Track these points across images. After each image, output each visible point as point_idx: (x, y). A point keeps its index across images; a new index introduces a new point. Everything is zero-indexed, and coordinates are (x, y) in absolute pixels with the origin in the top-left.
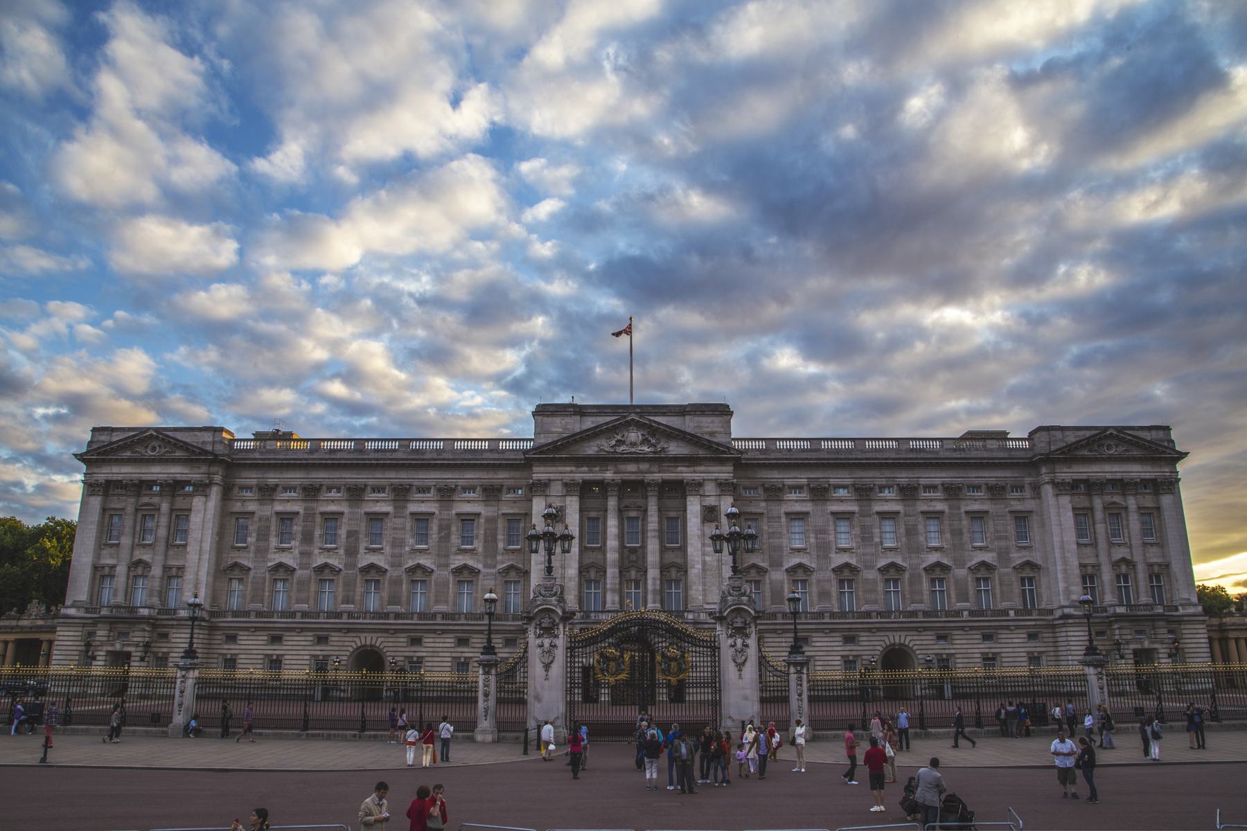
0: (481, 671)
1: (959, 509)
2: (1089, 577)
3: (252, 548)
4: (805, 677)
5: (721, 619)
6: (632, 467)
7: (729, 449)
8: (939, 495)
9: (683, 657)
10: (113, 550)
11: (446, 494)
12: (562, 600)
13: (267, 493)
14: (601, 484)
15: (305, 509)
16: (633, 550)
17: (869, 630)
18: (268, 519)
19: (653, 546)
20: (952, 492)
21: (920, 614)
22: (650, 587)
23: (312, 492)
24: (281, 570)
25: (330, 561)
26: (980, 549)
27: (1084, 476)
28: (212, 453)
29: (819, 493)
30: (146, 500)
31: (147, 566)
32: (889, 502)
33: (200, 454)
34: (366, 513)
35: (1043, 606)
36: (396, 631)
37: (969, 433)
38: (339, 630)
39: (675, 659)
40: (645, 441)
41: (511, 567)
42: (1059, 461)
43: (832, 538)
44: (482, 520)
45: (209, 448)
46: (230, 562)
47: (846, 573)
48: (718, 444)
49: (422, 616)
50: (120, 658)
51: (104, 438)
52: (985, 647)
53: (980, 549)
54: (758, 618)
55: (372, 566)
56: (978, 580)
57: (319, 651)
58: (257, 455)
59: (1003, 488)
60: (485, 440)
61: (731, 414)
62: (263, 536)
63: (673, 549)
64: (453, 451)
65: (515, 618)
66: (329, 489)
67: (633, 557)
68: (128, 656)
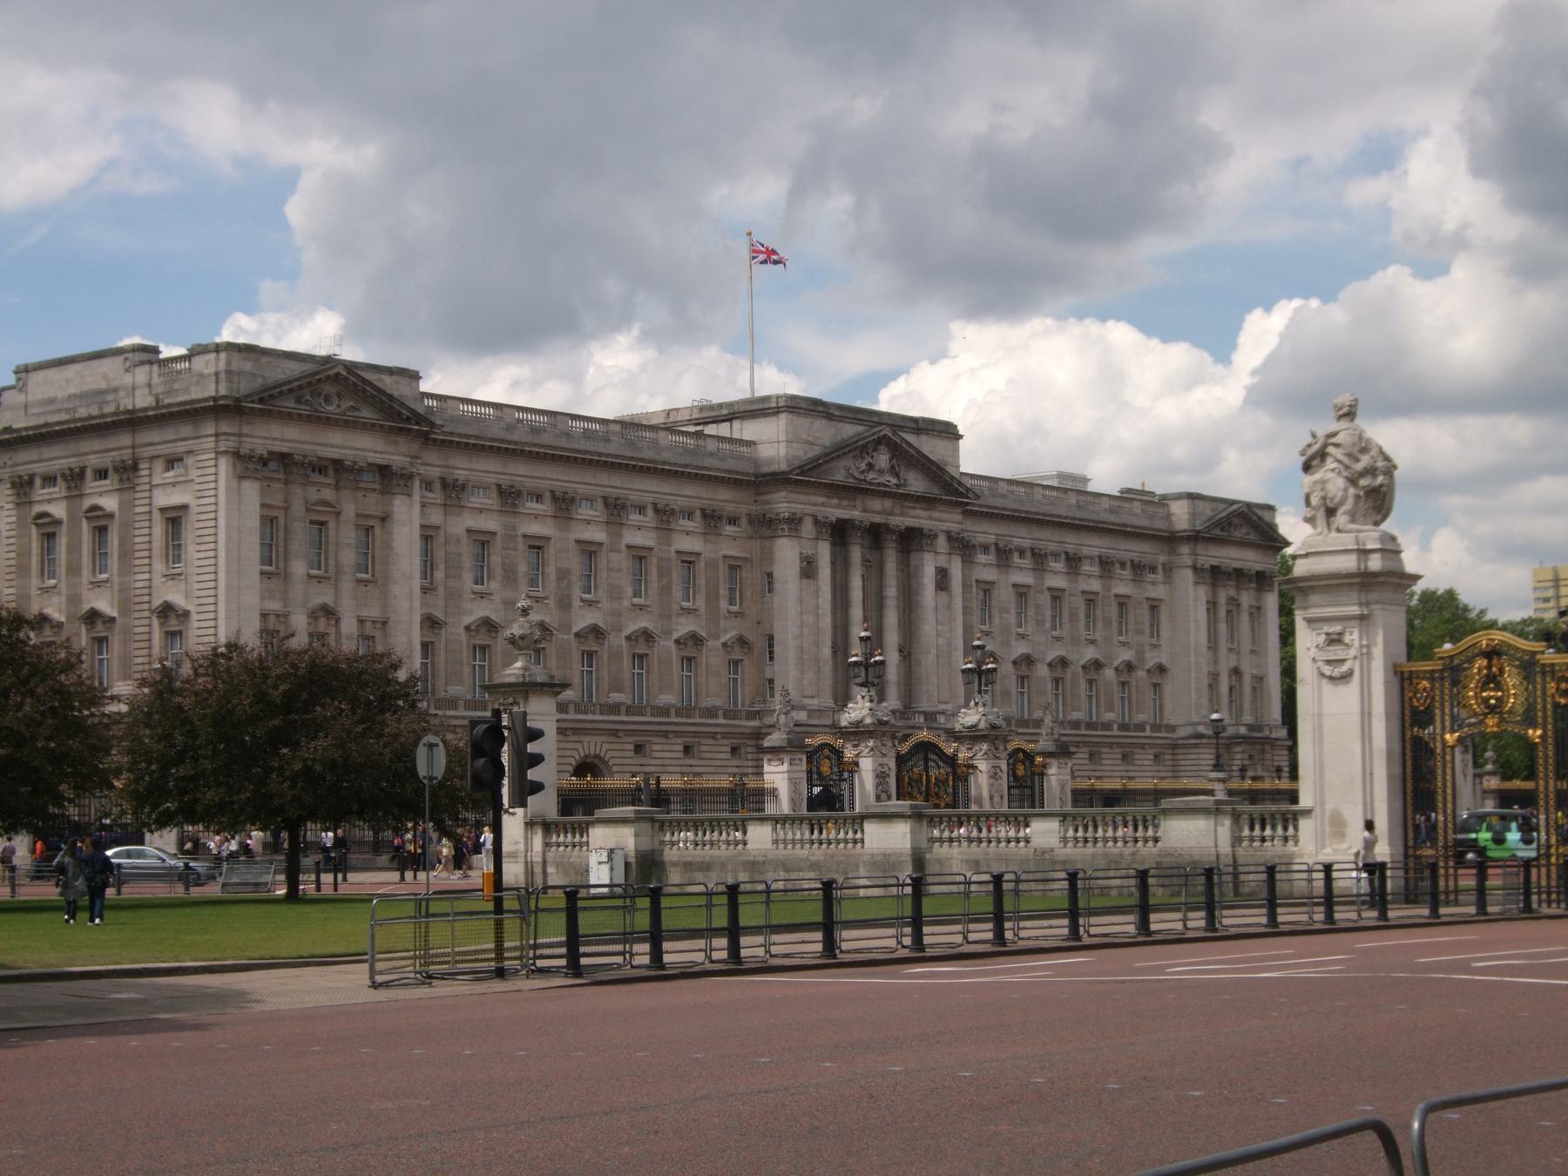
6: (876, 504)
10: (274, 584)
11: (665, 516)
13: (453, 490)
18: (458, 541)
19: (891, 619)
24: (483, 630)
26: (1124, 644)
27: (1215, 562)
29: (1004, 555)
33: (408, 420)
34: (578, 542)
44: (703, 565)
47: (1024, 667)
53: (1124, 644)
62: (453, 571)
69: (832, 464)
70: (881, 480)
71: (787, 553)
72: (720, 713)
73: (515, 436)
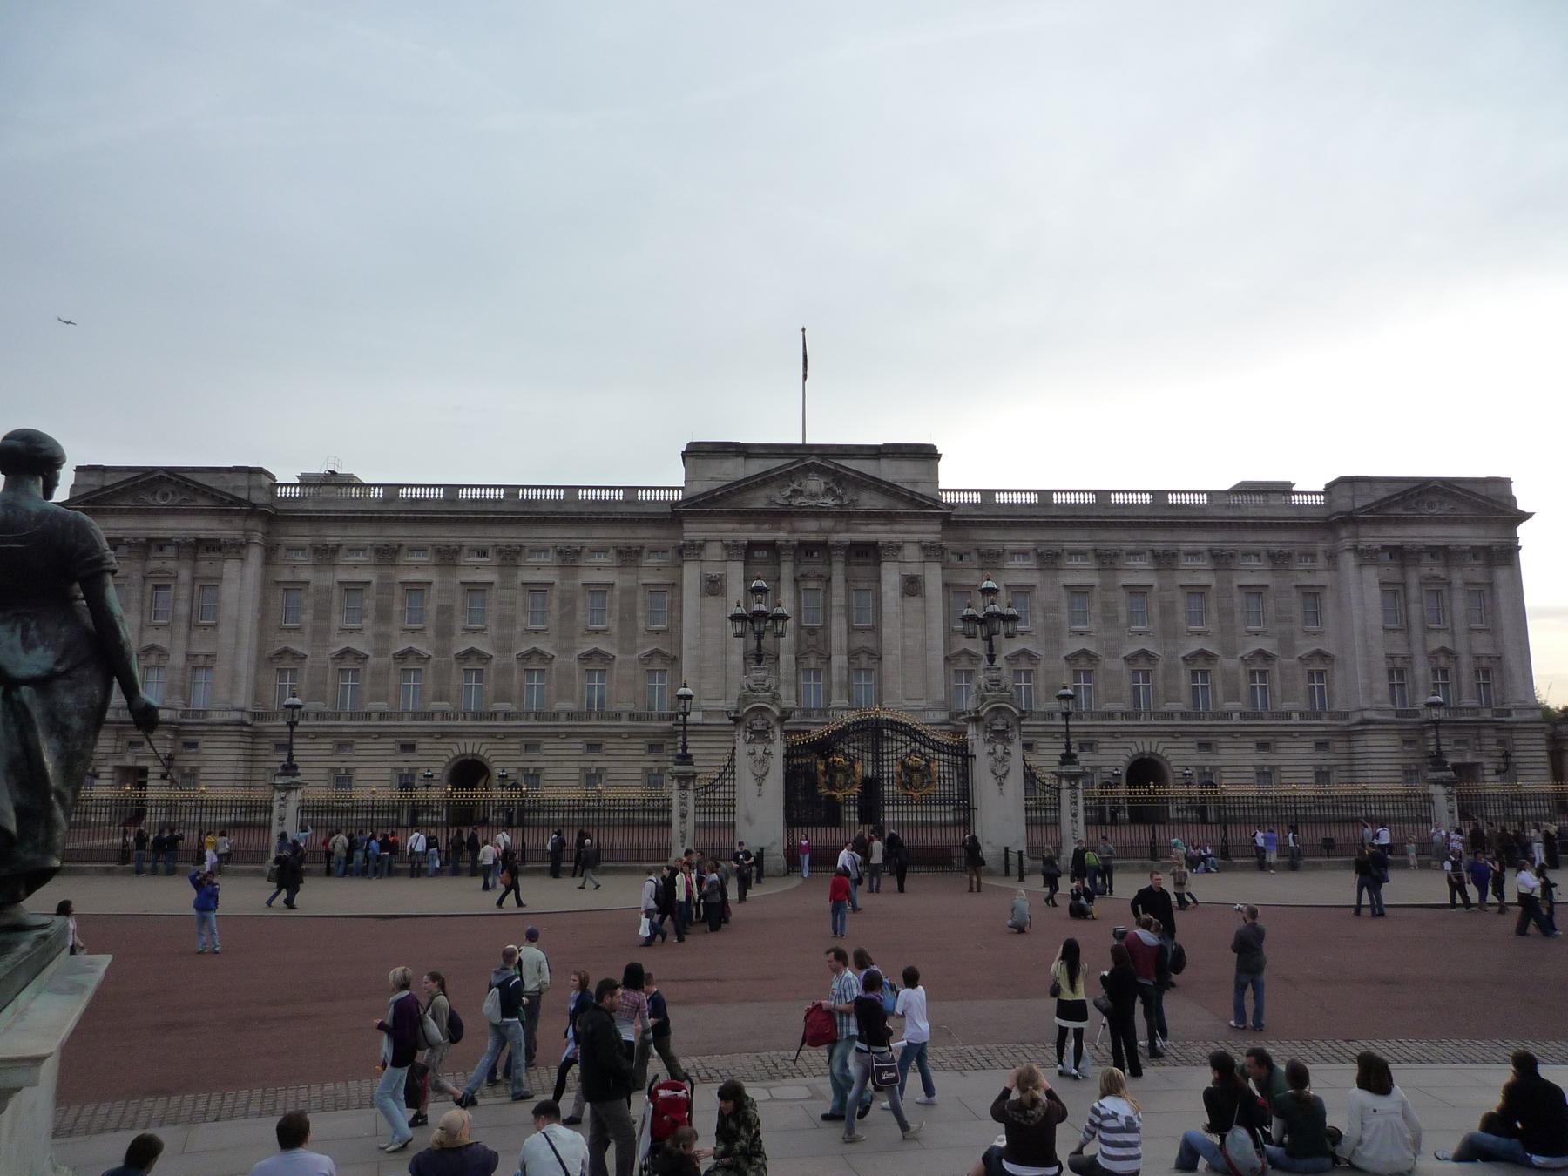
0: (675, 785)
1: (1230, 582)
2: (1398, 672)
3: (308, 629)
4: (1080, 794)
5: (976, 720)
6: (812, 524)
7: (937, 502)
8: (1204, 563)
9: (927, 766)
11: (569, 557)
12: (775, 697)
13: (326, 555)
14: (771, 546)
15: (381, 577)
16: (812, 631)
17: (1112, 735)
18: (328, 590)
19: (838, 627)
20: (1222, 560)
21: (1177, 716)
22: (835, 679)
23: (387, 554)
24: (349, 658)
25: (414, 646)
26: (1257, 633)
28: (248, 502)
29: (1049, 560)
30: (155, 564)
31: (162, 653)
32: (1139, 573)
35: (1337, 707)
36: (506, 735)
37: (1243, 484)
38: (430, 735)
39: (917, 770)
40: (829, 491)
41: (656, 652)
42: (1364, 521)
43: (1064, 617)
44: (617, 593)
45: (243, 495)
46: (278, 648)
47: (1083, 662)
48: (922, 496)
49: (538, 716)
50: (138, 776)
51: (94, 481)
52: (1259, 758)
53: (1257, 633)
54: (1022, 718)
55: (472, 651)
56: (1252, 673)
57: (404, 761)
58: (309, 506)
59: (1289, 555)
60: (619, 488)
61: (938, 457)
62: (322, 612)
63: (863, 630)
64: (577, 502)
65: (661, 717)
66: (412, 550)
67: (812, 640)
68: (143, 772)
69: (749, 495)
70: (813, 503)
71: (691, 574)
72: (625, 716)
73: (392, 507)
